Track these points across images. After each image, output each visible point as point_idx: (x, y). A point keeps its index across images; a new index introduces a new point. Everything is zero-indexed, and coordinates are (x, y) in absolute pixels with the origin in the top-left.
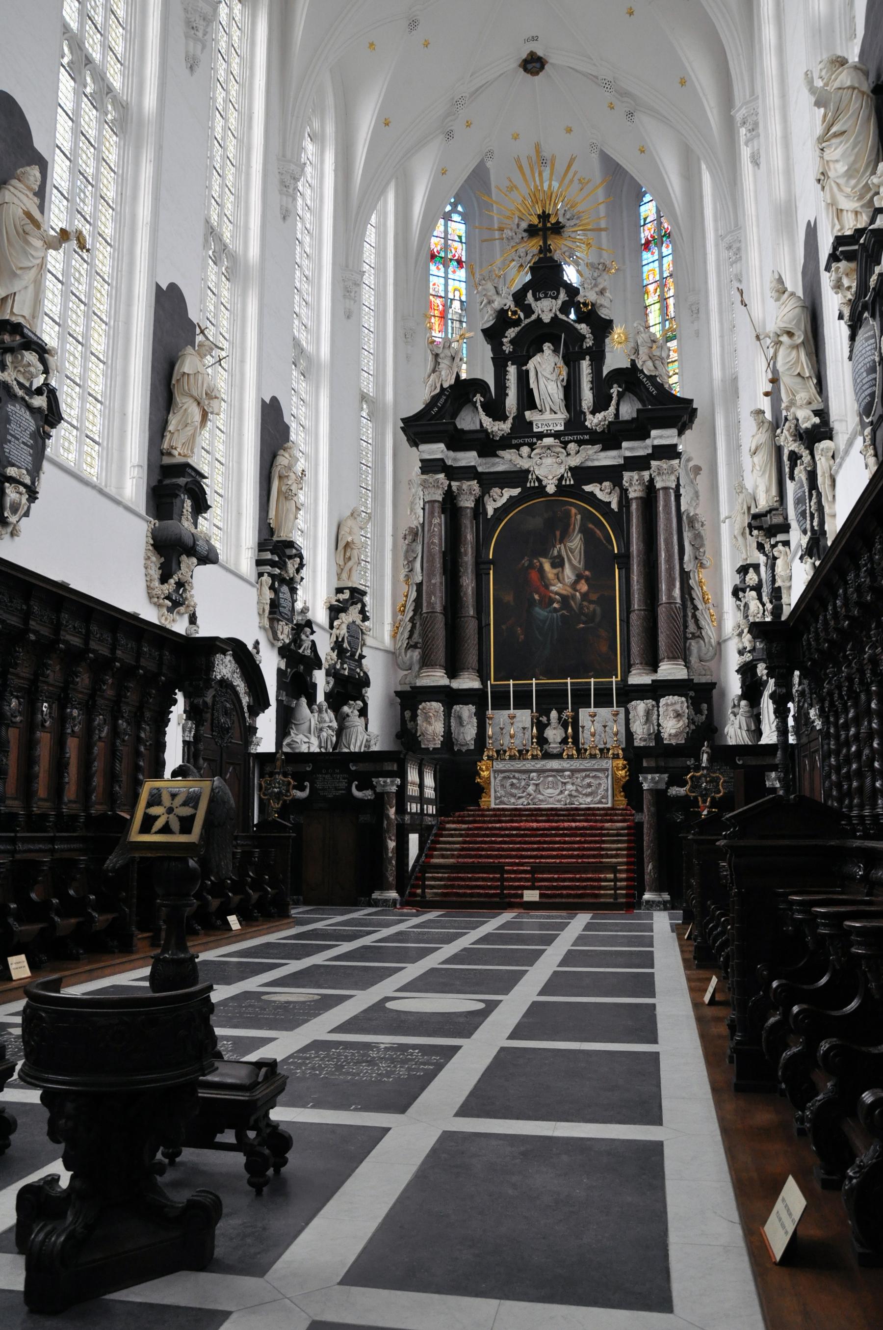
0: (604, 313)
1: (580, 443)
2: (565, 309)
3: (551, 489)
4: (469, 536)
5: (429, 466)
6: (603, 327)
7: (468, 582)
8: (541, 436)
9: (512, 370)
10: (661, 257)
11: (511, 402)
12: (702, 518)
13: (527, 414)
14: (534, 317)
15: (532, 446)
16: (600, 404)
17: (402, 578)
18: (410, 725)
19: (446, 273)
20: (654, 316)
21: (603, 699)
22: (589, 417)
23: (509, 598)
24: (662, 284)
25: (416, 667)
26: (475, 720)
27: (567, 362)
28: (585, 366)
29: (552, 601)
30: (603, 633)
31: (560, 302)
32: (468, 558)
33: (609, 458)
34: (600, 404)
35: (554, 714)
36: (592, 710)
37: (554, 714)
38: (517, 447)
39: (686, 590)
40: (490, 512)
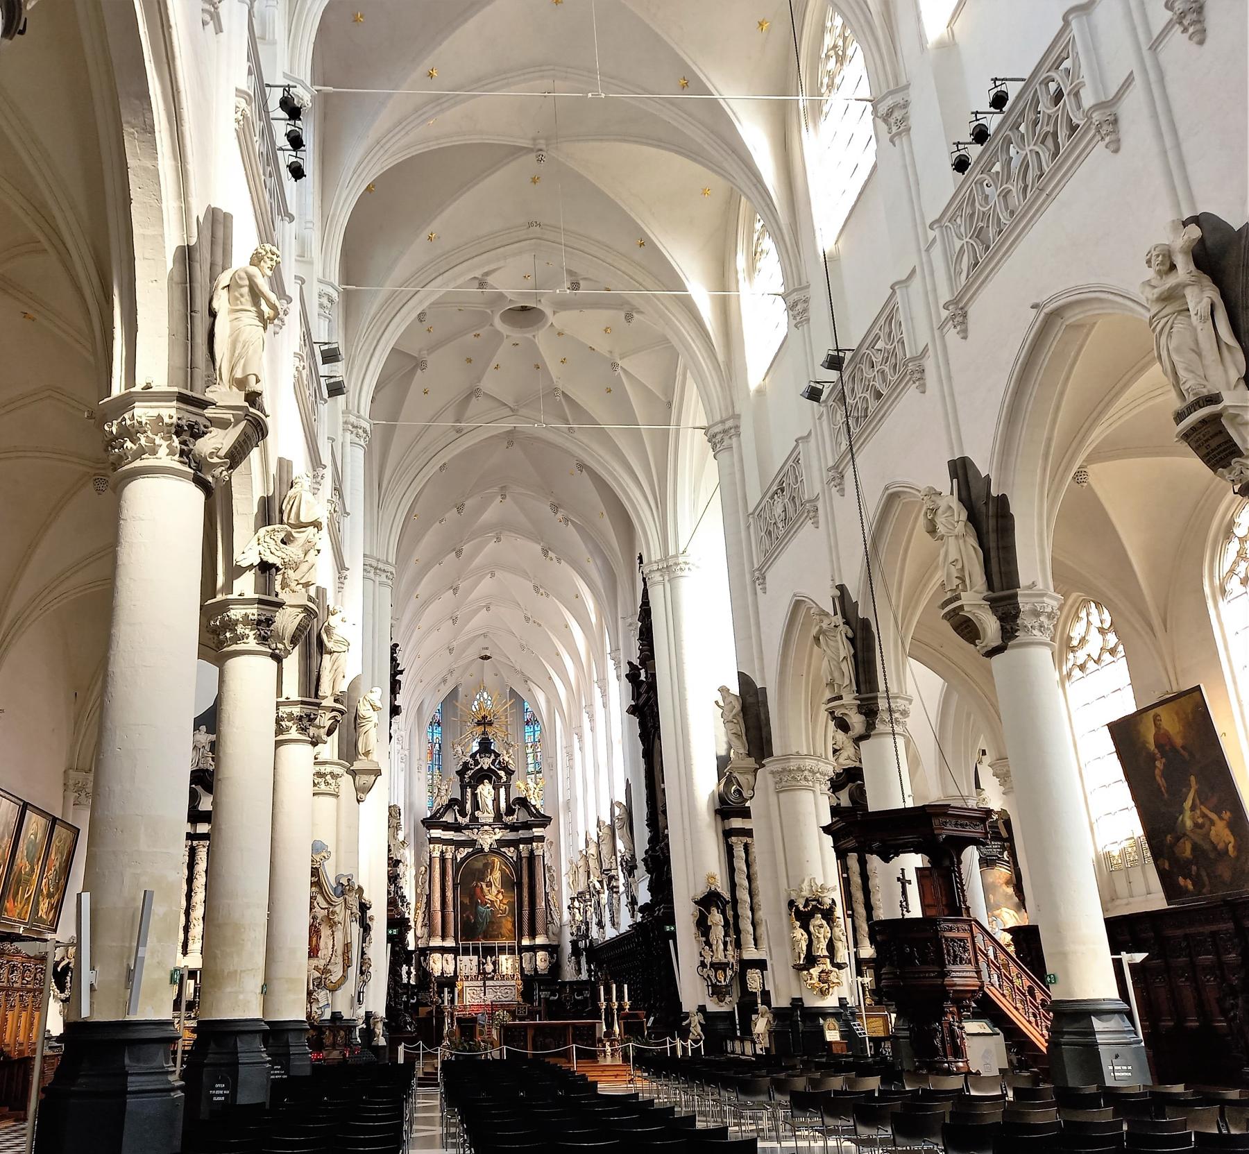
0: (511, 767)
1: (500, 829)
2: (493, 763)
3: (487, 849)
4: (451, 872)
5: (432, 840)
6: (510, 773)
7: (450, 894)
8: (482, 826)
9: (469, 790)
10: (534, 731)
11: (468, 806)
12: (554, 868)
13: (476, 813)
14: (479, 766)
15: (478, 829)
16: (510, 812)
17: (419, 891)
18: (424, 964)
19: (433, 730)
20: (530, 760)
21: (512, 951)
22: (505, 817)
23: (467, 901)
24: (534, 746)
25: (426, 935)
26: (454, 961)
27: (494, 788)
28: (502, 791)
29: (486, 903)
30: (509, 919)
31: (491, 759)
32: (450, 883)
33: (511, 836)
34: (510, 812)
35: (489, 957)
36: (507, 956)
37: (489, 957)
38: (472, 829)
39: (547, 901)
40: (459, 860)
